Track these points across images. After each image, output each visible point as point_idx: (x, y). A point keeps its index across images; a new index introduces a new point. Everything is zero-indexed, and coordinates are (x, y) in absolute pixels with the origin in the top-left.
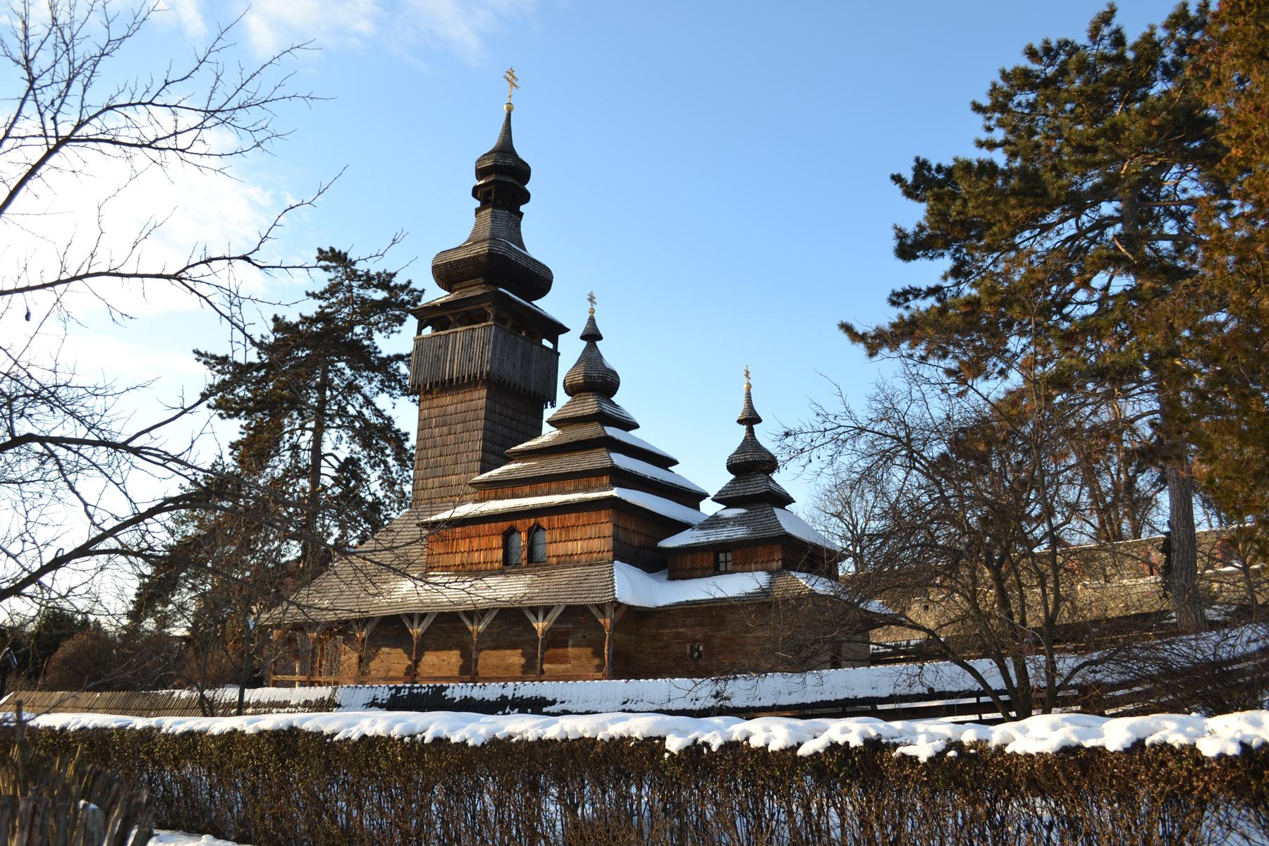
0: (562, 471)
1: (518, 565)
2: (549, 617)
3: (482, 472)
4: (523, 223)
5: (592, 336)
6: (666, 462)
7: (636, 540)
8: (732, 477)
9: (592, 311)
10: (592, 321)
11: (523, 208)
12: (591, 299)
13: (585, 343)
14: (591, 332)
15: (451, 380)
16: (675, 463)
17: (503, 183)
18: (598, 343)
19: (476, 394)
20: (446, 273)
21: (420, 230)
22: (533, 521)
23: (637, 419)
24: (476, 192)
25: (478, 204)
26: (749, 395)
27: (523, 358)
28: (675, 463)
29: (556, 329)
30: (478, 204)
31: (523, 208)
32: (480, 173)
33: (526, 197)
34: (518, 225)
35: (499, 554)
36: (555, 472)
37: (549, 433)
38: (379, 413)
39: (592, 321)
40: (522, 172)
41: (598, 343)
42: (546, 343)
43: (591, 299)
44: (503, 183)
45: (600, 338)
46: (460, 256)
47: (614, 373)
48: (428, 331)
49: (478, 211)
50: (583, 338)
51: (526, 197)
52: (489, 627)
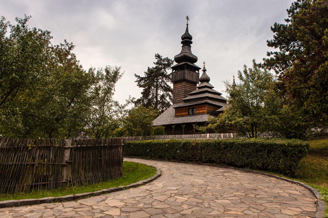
1: (191, 115)
3: (185, 97)
4: (191, 48)
5: (204, 71)
6: (219, 94)
7: (212, 110)
9: (204, 66)
10: (204, 67)
11: (191, 45)
12: (204, 63)
13: (203, 72)
15: (177, 81)
16: (222, 94)
17: (187, 40)
18: (206, 72)
19: (183, 83)
20: (177, 59)
21: (172, 50)
24: (182, 43)
25: (182, 45)
26: (234, 81)
27: (192, 75)
28: (222, 94)
29: (198, 69)
30: (182, 45)
31: (191, 45)
32: (182, 39)
33: (191, 43)
34: (190, 49)
35: (187, 113)
37: (197, 90)
38: (168, 86)
39: (204, 67)
40: (191, 38)
41: (206, 72)
42: (197, 72)
43: (204, 63)
44: (187, 40)
45: (206, 71)
46: (180, 56)
47: (209, 78)
48: (174, 71)
49: (182, 47)
50: (203, 71)
51: (191, 43)
52: (186, 126)
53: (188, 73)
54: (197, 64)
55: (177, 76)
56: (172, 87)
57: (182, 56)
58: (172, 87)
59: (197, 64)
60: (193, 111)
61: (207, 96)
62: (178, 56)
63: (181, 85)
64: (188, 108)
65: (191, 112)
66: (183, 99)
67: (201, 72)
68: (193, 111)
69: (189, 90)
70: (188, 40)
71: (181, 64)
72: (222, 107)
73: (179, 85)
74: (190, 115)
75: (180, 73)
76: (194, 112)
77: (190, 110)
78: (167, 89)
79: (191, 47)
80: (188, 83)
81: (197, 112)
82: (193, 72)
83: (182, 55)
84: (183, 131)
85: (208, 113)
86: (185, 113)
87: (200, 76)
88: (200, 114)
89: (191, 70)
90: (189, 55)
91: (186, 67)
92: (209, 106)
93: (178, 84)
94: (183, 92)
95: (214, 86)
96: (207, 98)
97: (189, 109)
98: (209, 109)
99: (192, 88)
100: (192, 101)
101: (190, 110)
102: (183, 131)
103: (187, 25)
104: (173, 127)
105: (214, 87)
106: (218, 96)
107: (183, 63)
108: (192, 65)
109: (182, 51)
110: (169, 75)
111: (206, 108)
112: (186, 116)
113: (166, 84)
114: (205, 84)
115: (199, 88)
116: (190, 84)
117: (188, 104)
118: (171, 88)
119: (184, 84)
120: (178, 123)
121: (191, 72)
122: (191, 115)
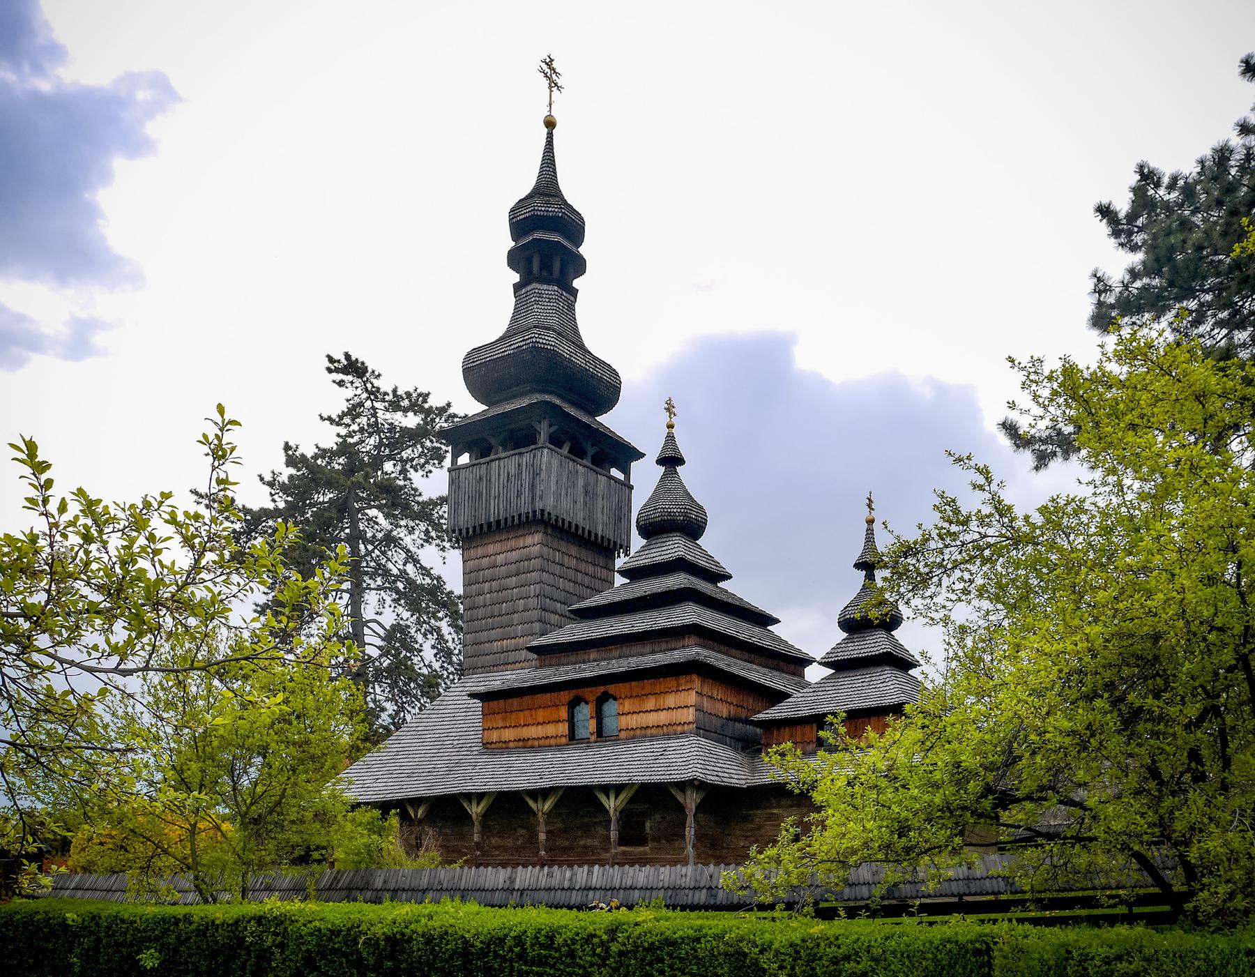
0: (635, 630)
1: (585, 740)
2: (622, 797)
5: (671, 461)
7: (724, 710)
8: (845, 635)
9: (670, 426)
10: (670, 438)
12: (670, 409)
14: (669, 453)
17: (547, 242)
19: (529, 540)
22: (602, 689)
23: (727, 566)
27: (586, 493)
29: (624, 454)
34: (571, 308)
35: (563, 728)
36: (626, 631)
39: (670, 438)
40: (572, 226)
43: (670, 409)
44: (547, 242)
49: (517, 288)
52: (556, 806)
53: (559, 475)
54: (612, 421)
55: (489, 488)
56: (455, 583)
57: (519, 352)
58: (455, 583)
59: (612, 421)
60: (599, 716)
61: (698, 621)
62: (489, 356)
63: (514, 555)
64: (565, 696)
65: (592, 725)
66: (535, 643)
67: (645, 478)
68: (599, 716)
69: (570, 587)
70: (556, 238)
71: (509, 407)
72: (788, 696)
73: (500, 552)
74: (582, 741)
75: (506, 465)
76: (610, 724)
77: (585, 712)
78: (423, 596)
79: (574, 293)
80: (563, 546)
81: (626, 722)
82: (592, 476)
83: (517, 341)
84: (542, 837)
85: (702, 730)
86: (550, 730)
87: (639, 499)
88: (652, 738)
89: (577, 452)
90: (565, 350)
91: (544, 430)
92: (706, 690)
93: (491, 549)
94: (533, 602)
95: (729, 570)
96: (693, 640)
97: (573, 704)
98: (706, 704)
99: (587, 580)
100: (593, 654)
101: (585, 712)
102: (542, 837)
103: (550, 124)
104: (476, 810)
105: (729, 577)
106: (757, 630)
107: (524, 402)
108: (585, 419)
109: (514, 319)
110: (433, 503)
111: (692, 698)
112: (559, 747)
113: (411, 558)
114: (674, 547)
115: (633, 574)
116: (574, 550)
117: (566, 673)
118: (448, 588)
119: (533, 542)
120: (505, 788)
121: (580, 468)
122: (585, 740)
